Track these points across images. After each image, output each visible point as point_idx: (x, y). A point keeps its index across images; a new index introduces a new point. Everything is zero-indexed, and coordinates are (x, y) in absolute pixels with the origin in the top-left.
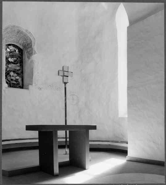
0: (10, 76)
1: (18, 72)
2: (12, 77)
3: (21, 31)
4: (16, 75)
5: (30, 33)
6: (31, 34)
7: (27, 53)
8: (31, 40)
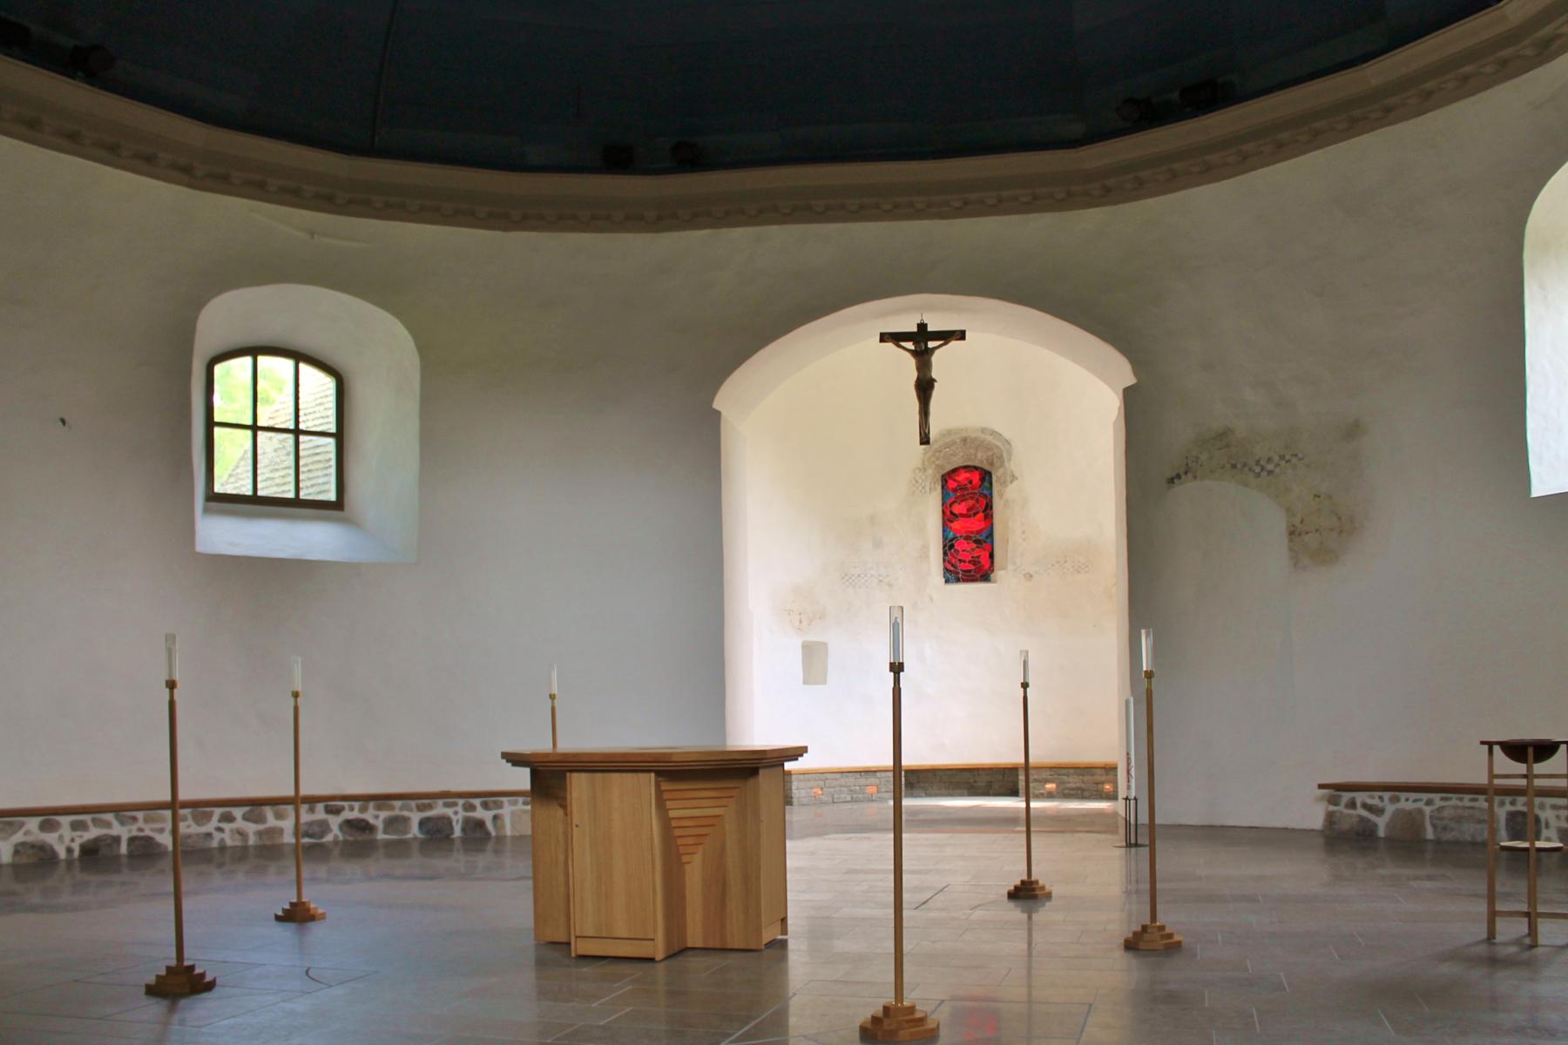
0: (957, 551)
1: (978, 537)
5: (994, 431)
8: (998, 447)
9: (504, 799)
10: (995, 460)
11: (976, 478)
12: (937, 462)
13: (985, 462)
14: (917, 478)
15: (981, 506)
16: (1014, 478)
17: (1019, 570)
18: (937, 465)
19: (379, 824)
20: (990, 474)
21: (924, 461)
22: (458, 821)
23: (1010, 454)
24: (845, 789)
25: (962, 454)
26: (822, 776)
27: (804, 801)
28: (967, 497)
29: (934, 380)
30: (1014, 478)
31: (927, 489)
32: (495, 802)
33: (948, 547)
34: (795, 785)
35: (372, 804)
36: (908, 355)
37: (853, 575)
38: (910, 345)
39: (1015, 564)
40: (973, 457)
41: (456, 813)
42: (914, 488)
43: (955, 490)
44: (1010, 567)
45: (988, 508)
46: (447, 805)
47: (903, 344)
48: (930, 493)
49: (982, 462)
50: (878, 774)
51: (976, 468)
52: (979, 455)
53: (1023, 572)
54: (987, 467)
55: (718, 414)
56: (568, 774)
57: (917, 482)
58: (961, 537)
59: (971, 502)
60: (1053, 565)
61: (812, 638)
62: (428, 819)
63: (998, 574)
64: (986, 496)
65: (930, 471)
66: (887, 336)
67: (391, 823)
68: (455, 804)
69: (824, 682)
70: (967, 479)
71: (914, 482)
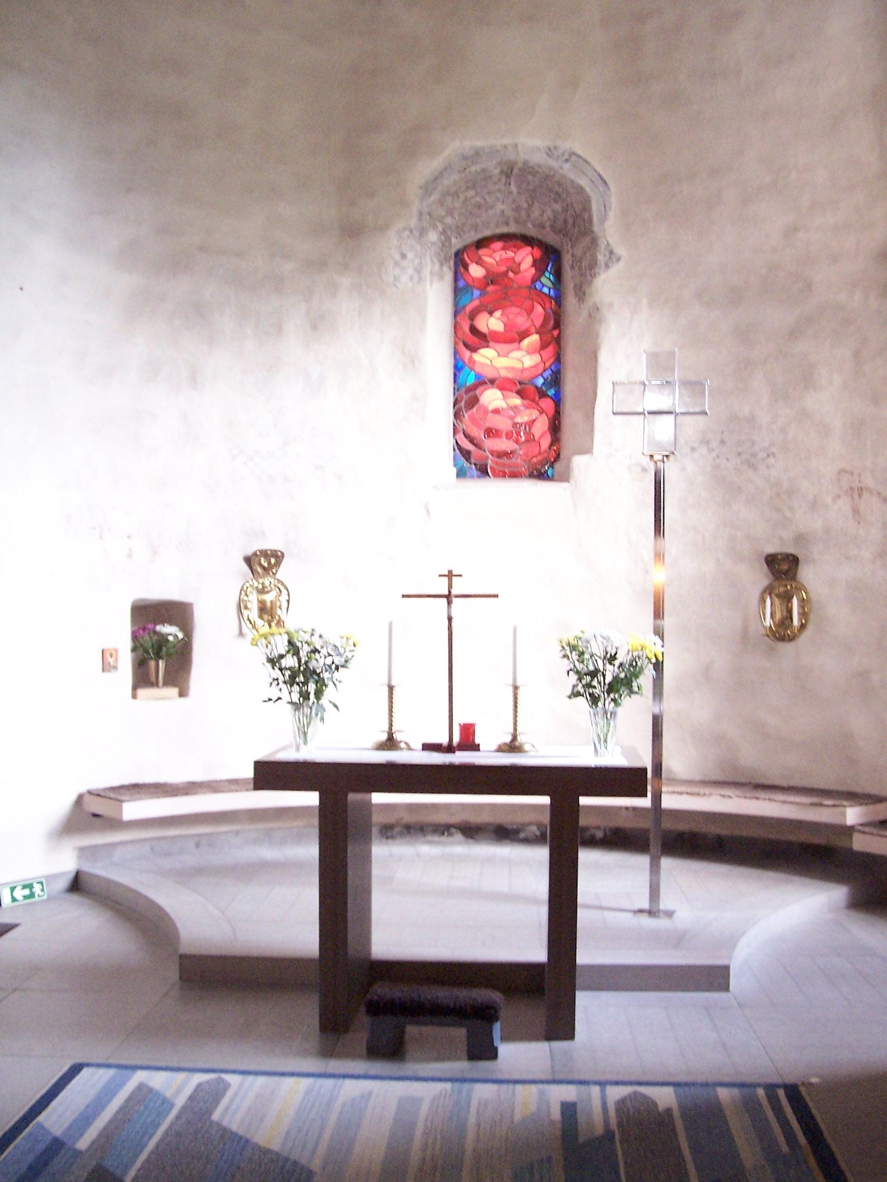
2: (490, 415)
3: (520, 165)
4: (517, 401)
6: (580, 157)
7: (572, 267)
8: (581, 190)
51: (527, 240)
57: (404, 256)
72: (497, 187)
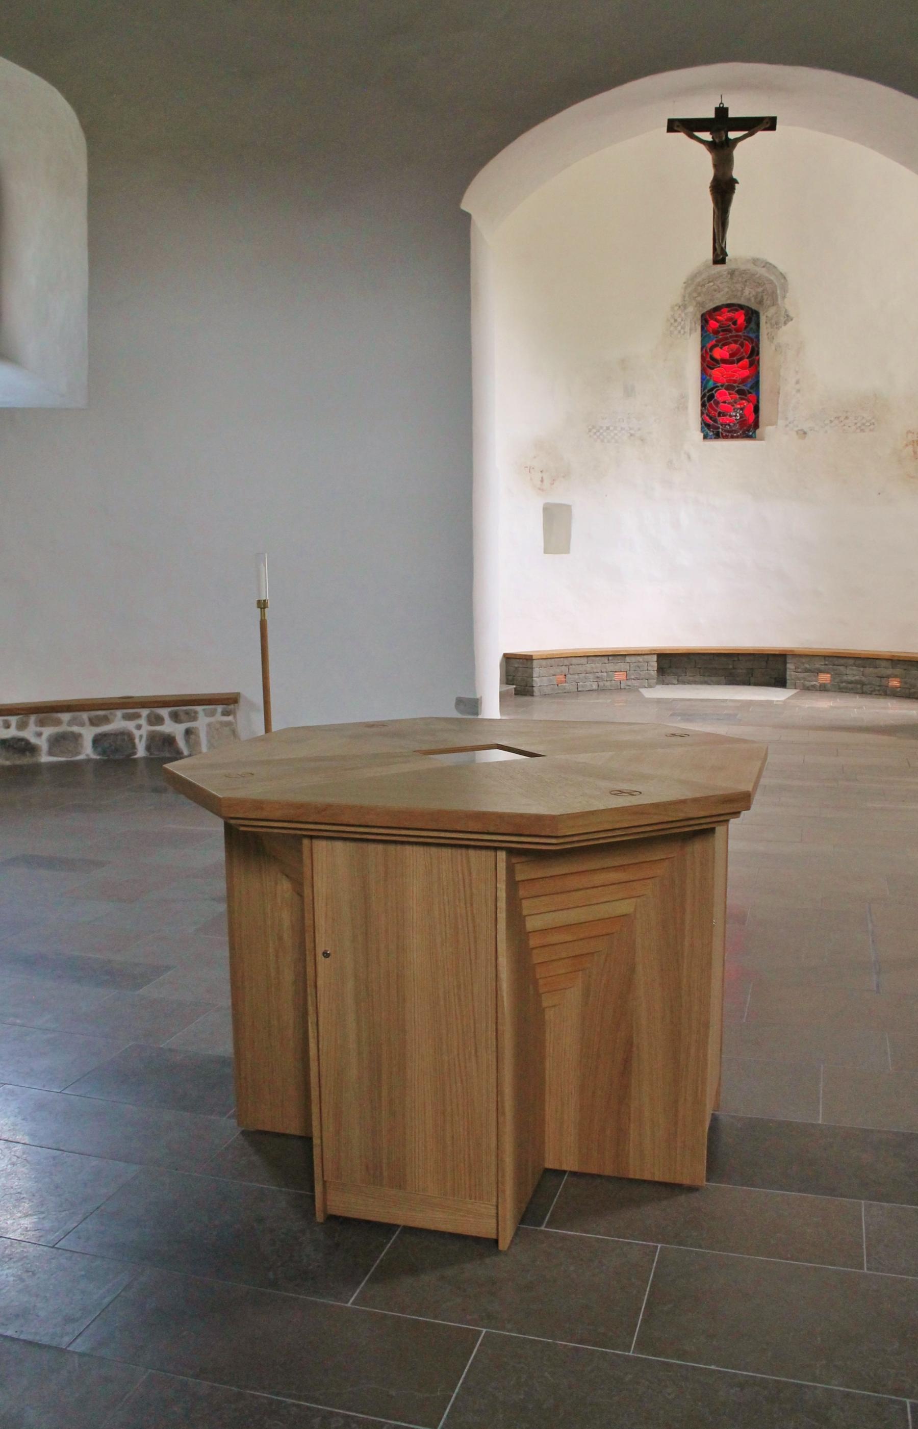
0: (717, 403)
1: (742, 387)
5: (767, 263)
6: (770, 264)
8: (771, 282)
9: (199, 708)
10: (765, 297)
11: (741, 320)
12: (699, 299)
13: (753, 299)
14: (676, 316)
15: (746, 352)
16: (788, 318)
17: (791, 425)
18: (698, 303)
19: (42, 743)
20: (756, 314)
21: (684, 297)
22: (141, 737)
23: (785, 290)
24: (591, 676)
25: (726, 290)
26: (566, 662)
27: (547, 691)
28: (730, 340)
29: (736, 181)
30: (788, 318)
31: (687, 329)
32: (187, 713)
33: (708, 398)
34: (536, 672)
35: (33, 718)
36: (703, 148)
37: (601, 427)
38: (707, 136)
39: (787, 419)
40: (739, 294)
41: (139, 727)
42: (672, 328)
43: (716, 333)
44: (781, 423)
45: (754, 353)
46: (127, 717)
47: (697, 134)
48: (690, 334)
49: (749, 299)
50: (628, 659)
51: (741, 307)
52: (747, 291)
53: (796, 429)
54: (754, 306)
55: (467, 217)
56: (306, 842)
57: (676, 321)
58: (722, 386)
59: (735, 346)
60: (831, 422)
61: (555, 499)
62: (104, 736)
63: (766, 429)
64: (751, 340)
65: (691, 309)
66: (677, 123)
67: (58, 742)
68: (138, 716)
69: (567, 551)
70: (730, 319)
71: (672, 321)
72: (726, 280)
